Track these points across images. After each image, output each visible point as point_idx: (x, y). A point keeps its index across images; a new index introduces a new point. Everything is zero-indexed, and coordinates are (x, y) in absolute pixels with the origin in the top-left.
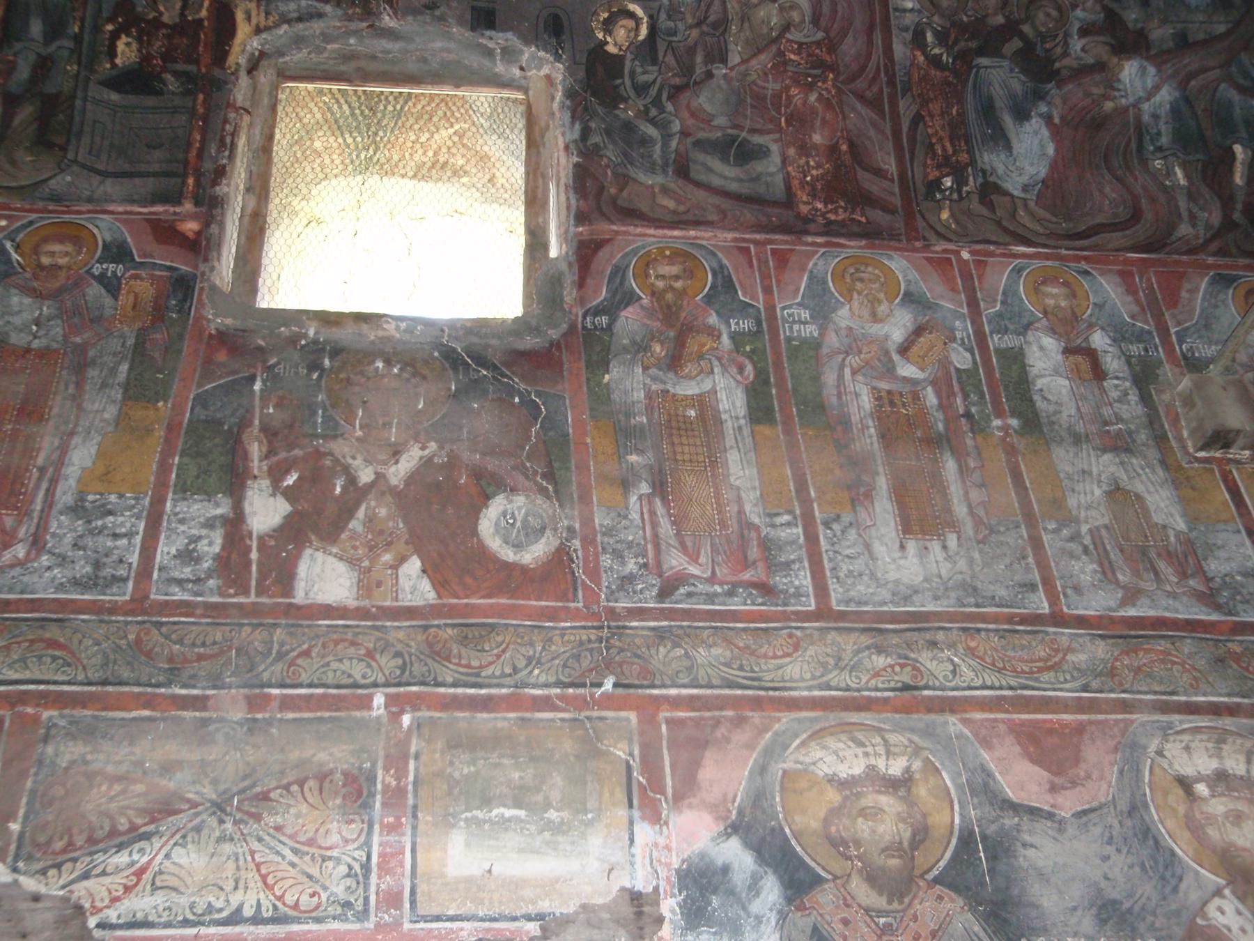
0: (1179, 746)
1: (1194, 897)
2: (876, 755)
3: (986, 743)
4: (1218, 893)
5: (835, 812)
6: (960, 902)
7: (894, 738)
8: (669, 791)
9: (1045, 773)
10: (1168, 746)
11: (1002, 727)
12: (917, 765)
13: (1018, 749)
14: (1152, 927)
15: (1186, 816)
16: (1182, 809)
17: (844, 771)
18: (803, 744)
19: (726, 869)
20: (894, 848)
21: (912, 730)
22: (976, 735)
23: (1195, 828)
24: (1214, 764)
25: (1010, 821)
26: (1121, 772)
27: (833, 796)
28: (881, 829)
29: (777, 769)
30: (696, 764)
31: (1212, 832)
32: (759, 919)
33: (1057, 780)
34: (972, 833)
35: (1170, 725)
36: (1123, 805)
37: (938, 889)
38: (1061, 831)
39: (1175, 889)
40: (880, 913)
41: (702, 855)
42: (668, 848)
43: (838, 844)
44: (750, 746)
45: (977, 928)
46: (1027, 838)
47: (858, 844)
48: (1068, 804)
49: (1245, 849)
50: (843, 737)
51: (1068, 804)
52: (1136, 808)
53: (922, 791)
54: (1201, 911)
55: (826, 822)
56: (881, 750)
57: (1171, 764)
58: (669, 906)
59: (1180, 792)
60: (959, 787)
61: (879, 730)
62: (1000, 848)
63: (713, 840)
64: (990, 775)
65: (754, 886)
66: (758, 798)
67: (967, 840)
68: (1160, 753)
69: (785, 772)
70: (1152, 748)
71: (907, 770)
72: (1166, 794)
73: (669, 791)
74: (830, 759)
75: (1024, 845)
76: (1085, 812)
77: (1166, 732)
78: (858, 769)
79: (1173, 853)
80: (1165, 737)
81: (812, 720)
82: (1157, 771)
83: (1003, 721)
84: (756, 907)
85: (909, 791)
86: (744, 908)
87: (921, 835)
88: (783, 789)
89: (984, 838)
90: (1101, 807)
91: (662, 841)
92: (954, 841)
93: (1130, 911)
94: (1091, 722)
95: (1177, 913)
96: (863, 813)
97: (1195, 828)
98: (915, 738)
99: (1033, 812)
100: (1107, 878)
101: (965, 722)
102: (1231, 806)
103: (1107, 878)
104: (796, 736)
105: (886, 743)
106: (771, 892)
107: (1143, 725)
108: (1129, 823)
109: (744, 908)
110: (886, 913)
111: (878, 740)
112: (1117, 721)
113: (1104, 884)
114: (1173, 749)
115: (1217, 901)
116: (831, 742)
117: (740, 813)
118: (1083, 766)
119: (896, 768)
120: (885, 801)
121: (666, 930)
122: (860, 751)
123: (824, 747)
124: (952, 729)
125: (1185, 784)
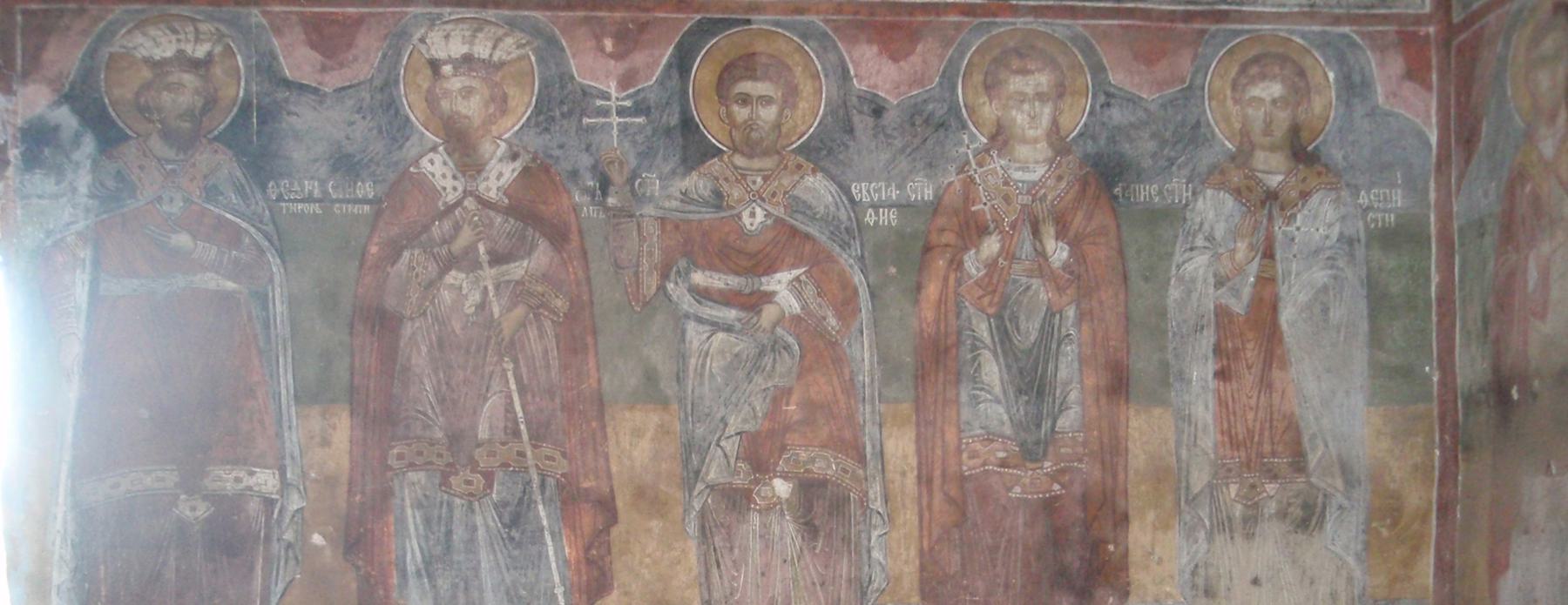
0: (441, 33)
1: (414, 152)
2: (188, 41)
3: (278, 32)
4: (434, 149)
5: (147, 86)
6: (230, 153)
7: (204, 27)
8: (19, 68)
9: (319, 57)
10: (431, 34)
11: (294, 18)
12: (218, 49)
13: (303, 37)
14: (373, 174)
15: (428, 91)
16: (425, 85)
17: (158, 54)
18: (129, 32)
19: (57, 128)
20: (189, 114)
21: (220, 20)
22: (271, 24)
23: (431, 101)
24: (465, 49)
25: (282, 94)
26: (384, 56)
27: (147, 74)
28: (181, 99)
29: (105, 52)
30: (40, 48)
31: (445, 105)
32: (77, 164)
33: (329, 63)
34: (250, 104)
35: (440, 16)
36: (377, 83)
37: (216, 145)
38: (321, 102)
39: (401, 147)
40: (168, 161)
41: (41, 118)
42: (15, 112)
43: (144, 110)
44: (85, 33)
45: (239, 174)
46: (292, 108)
47: (159, 110)
48: (332, 81)
49: (466, 117)
50: (162, 26)
51: (332, 81)
52: (389, 84)
53: (217, 71)
54: (416, 163)
55: (138, 95)
56: (191, 37)
57: (428, 50)
58: (14, 154)
59: (429, 72)
60: (248, 68)
61: (193, 20)
62: (268, 115)
63: (49, 107)
64: (275, 58)
65: (76, 141)
66: (87, 74)
67: (246, 107)
68: (422, 40)
69: (111, 55)
70: (418, 35)
71: (210, 54)
72: (417, 72)
73: (19, 68)
74: (149, 44)
75: (289, 114)
76: (343, 88)
77: (433, 21)
78: (169, 53)
79: (408, 119)
80: (432, 26)
81: (143, 11)
82: (415, 54)
83: (296, 13)
84: (76, 156)
85: (208, 70)
86: (68, 157)
87: (211, 102)
88: (108, 67)
89: (259, 108)
90: (359, 84)
91: (10, 107)
92: (235, 110)
93: (359, 162)
94: (371, 15)
95: (396, 163)
96: (169, 87)
97: (431, 101)
98: (223, 28)
99: (302, 88)
100: (348, 138)
101: (265, 13)
102: (467, 83)
103: (348, 138)
104: (124, 25)
105: (196, 30)
106: (89, 145)
107: (415, 16)
108: (379, 96)
109: (68, 157)
110: (174, 161)
111: (191, 28)
112: (393, 13)
113: (345, 142)
114: (435, 37)
115: (431, 155)
116: (153, 31)
117: (72, 88)
118: (354, 51)
119: (201, 51)
120: (189, 79)
121: (10, 172)
122: (174, 38)
123: (145, 34)
124: (254, 20)
125: (435, 65)
